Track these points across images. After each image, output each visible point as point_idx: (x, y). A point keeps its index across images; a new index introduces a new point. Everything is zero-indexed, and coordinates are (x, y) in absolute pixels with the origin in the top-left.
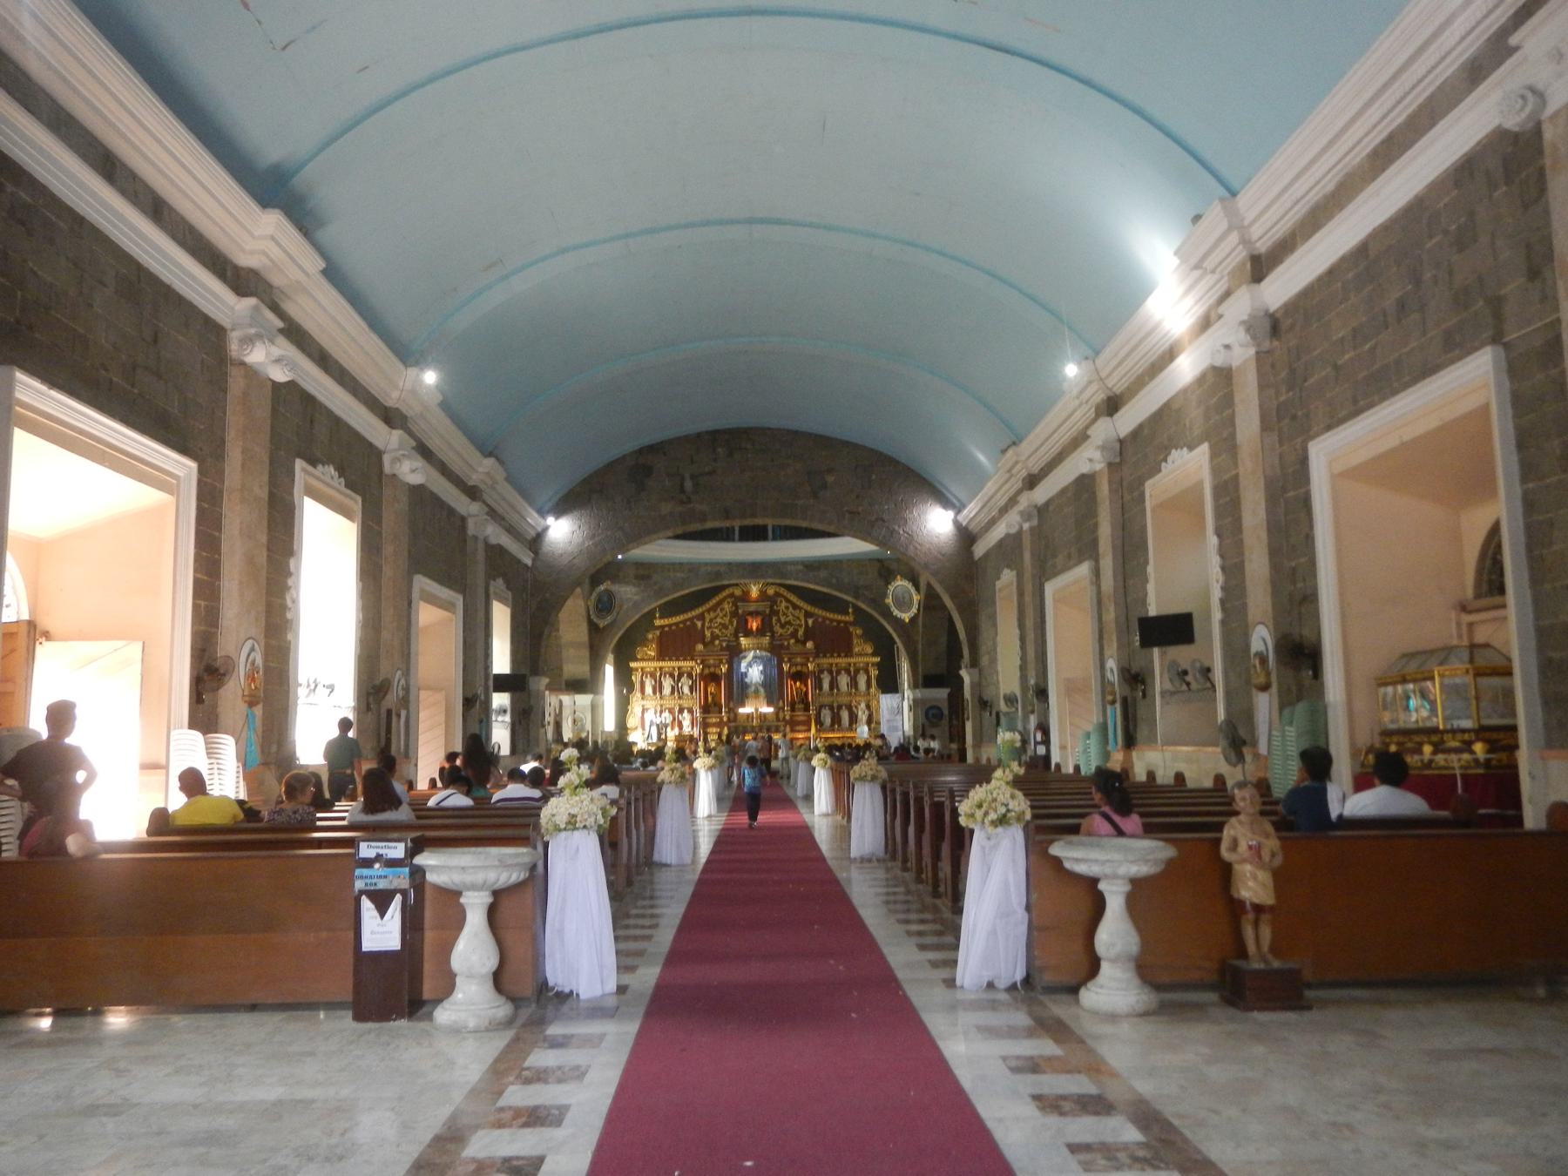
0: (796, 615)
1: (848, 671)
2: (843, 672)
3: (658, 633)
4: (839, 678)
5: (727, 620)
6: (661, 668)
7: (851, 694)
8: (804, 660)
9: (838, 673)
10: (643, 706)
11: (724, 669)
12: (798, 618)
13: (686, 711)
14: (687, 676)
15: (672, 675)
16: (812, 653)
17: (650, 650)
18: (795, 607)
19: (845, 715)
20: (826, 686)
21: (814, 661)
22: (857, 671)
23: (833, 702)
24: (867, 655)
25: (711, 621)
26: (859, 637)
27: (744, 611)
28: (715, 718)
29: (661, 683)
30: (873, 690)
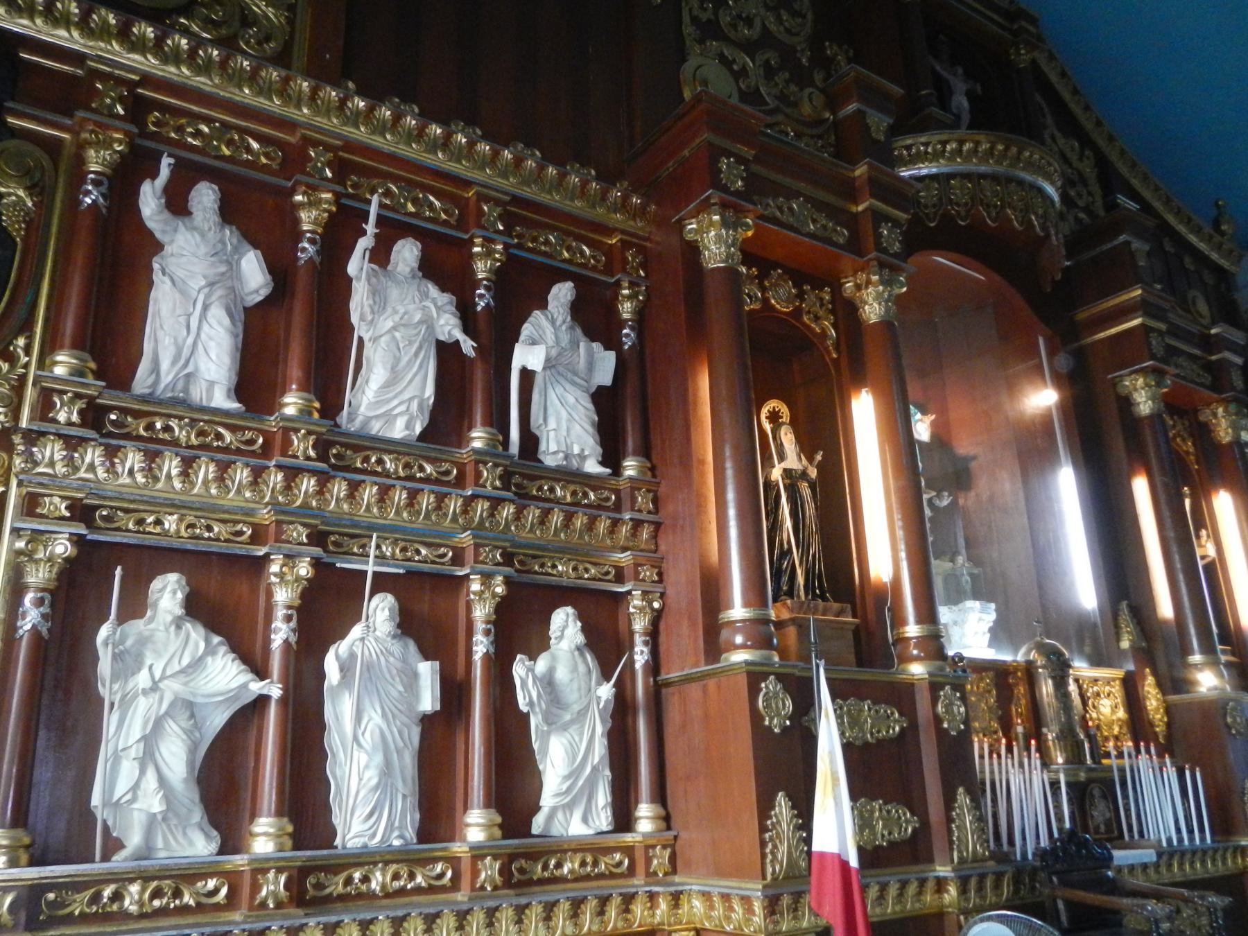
0: (1074, 158)
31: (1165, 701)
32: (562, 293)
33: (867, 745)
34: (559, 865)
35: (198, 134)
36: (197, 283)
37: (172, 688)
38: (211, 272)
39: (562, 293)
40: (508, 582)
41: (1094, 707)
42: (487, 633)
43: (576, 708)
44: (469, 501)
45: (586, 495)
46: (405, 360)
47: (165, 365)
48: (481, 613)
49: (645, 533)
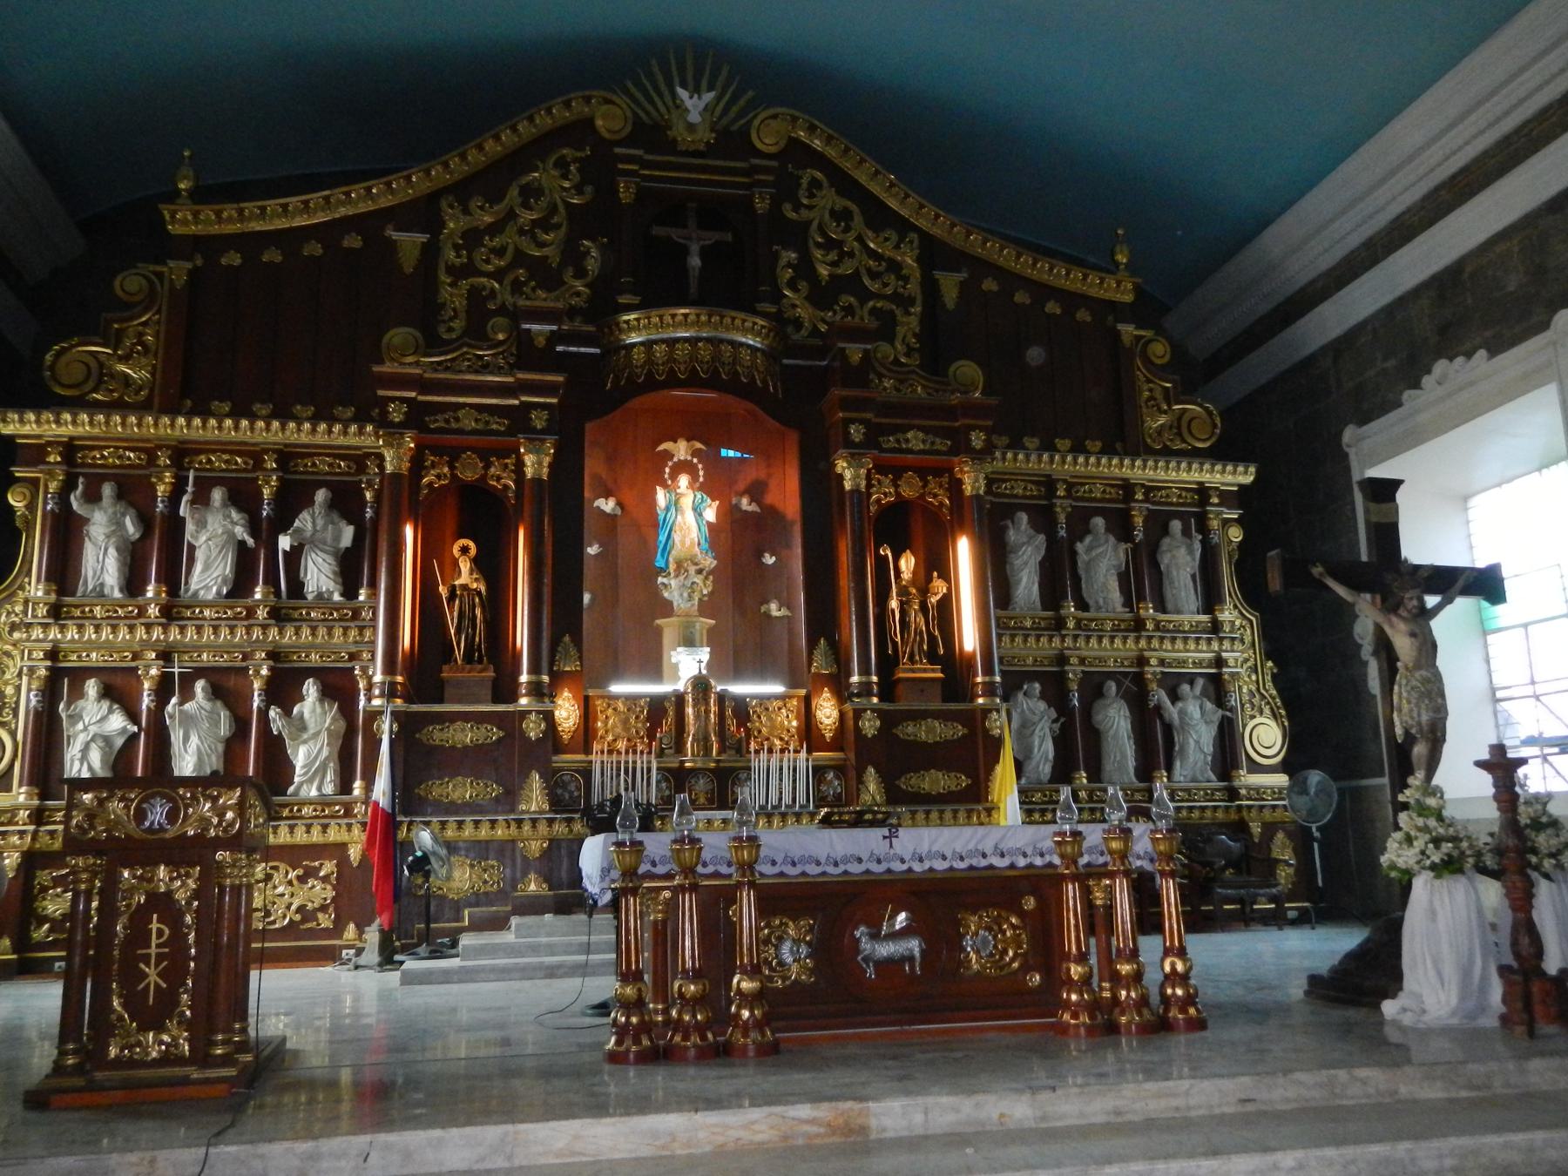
1: (1121, 527)
2: (1099, 522)
3: (178, 271)
4: (1080, 547)
5: (549, 248)
6: (182, 453)
7: (1138, 625)
8: (942, 444)
9: (1080, 525)
10: (53, 654)
11: (535, 463)
12: (895, 267)
13: (310, 689)
14: (334, 505)
15: (242, 497)
16: (971, 409)
17: (125, 359)
18: (879, 216)
19: (1117, 721)
20: (1027, 586)
21: (988, 451)
22: (1159, 524)
23: (1062, 659)
24: (1194, 454)
25: (472, 238)
26: (1161, 371)
27: (642, 195)
28: (479, 718)
29: (175, 526)
30: (1227, 615)
31: (840, 711)
32: (321, 495)
33: (466, 747)
34: (299, 810)
35: (103, 457)
36: (101, 538)
37: (93, 729)
38: (107, 531)
39: (321, 495)
40: (271, 669)
41: (759, 717)
42: (259, 695)
43: (311, 731)
44: (249, 629)
45: (332, 614)
46: (214, 555)
47: (90, 580)
48: (257, 685)
49: (368, 633)
